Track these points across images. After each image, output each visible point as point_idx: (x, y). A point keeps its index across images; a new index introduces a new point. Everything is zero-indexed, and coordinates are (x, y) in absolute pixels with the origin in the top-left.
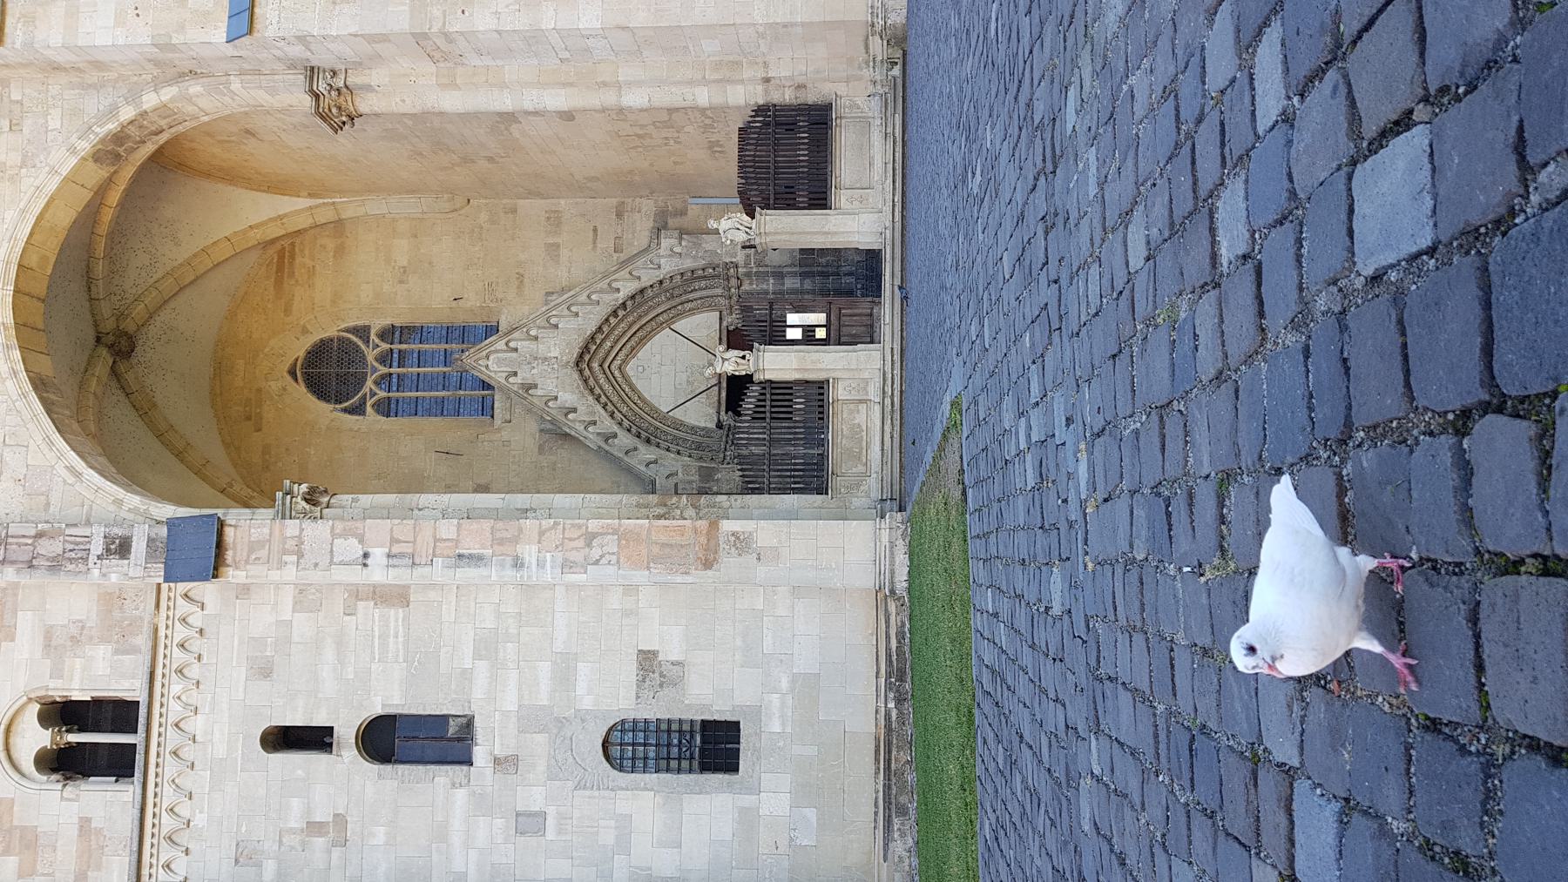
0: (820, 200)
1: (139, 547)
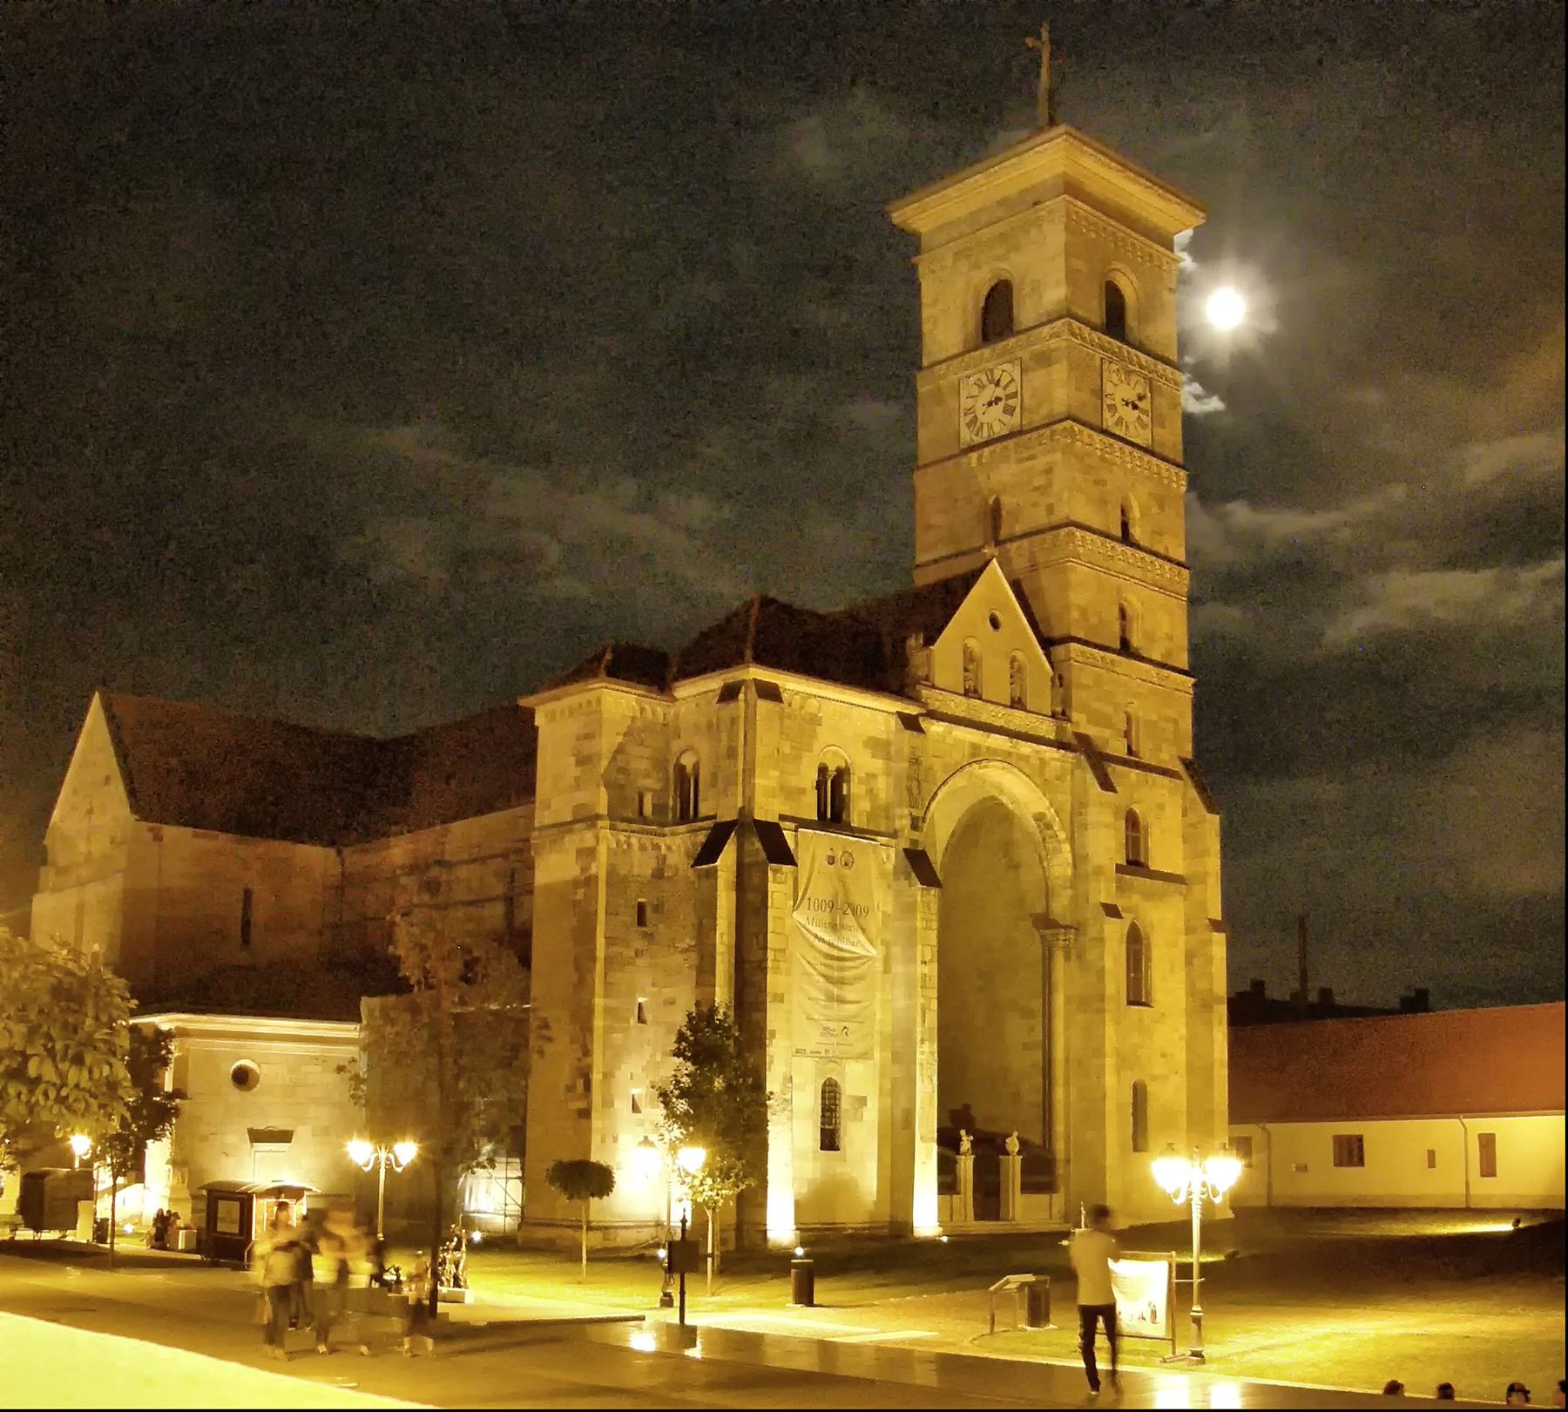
0: (1027, 1188)
1: (916, 835)
